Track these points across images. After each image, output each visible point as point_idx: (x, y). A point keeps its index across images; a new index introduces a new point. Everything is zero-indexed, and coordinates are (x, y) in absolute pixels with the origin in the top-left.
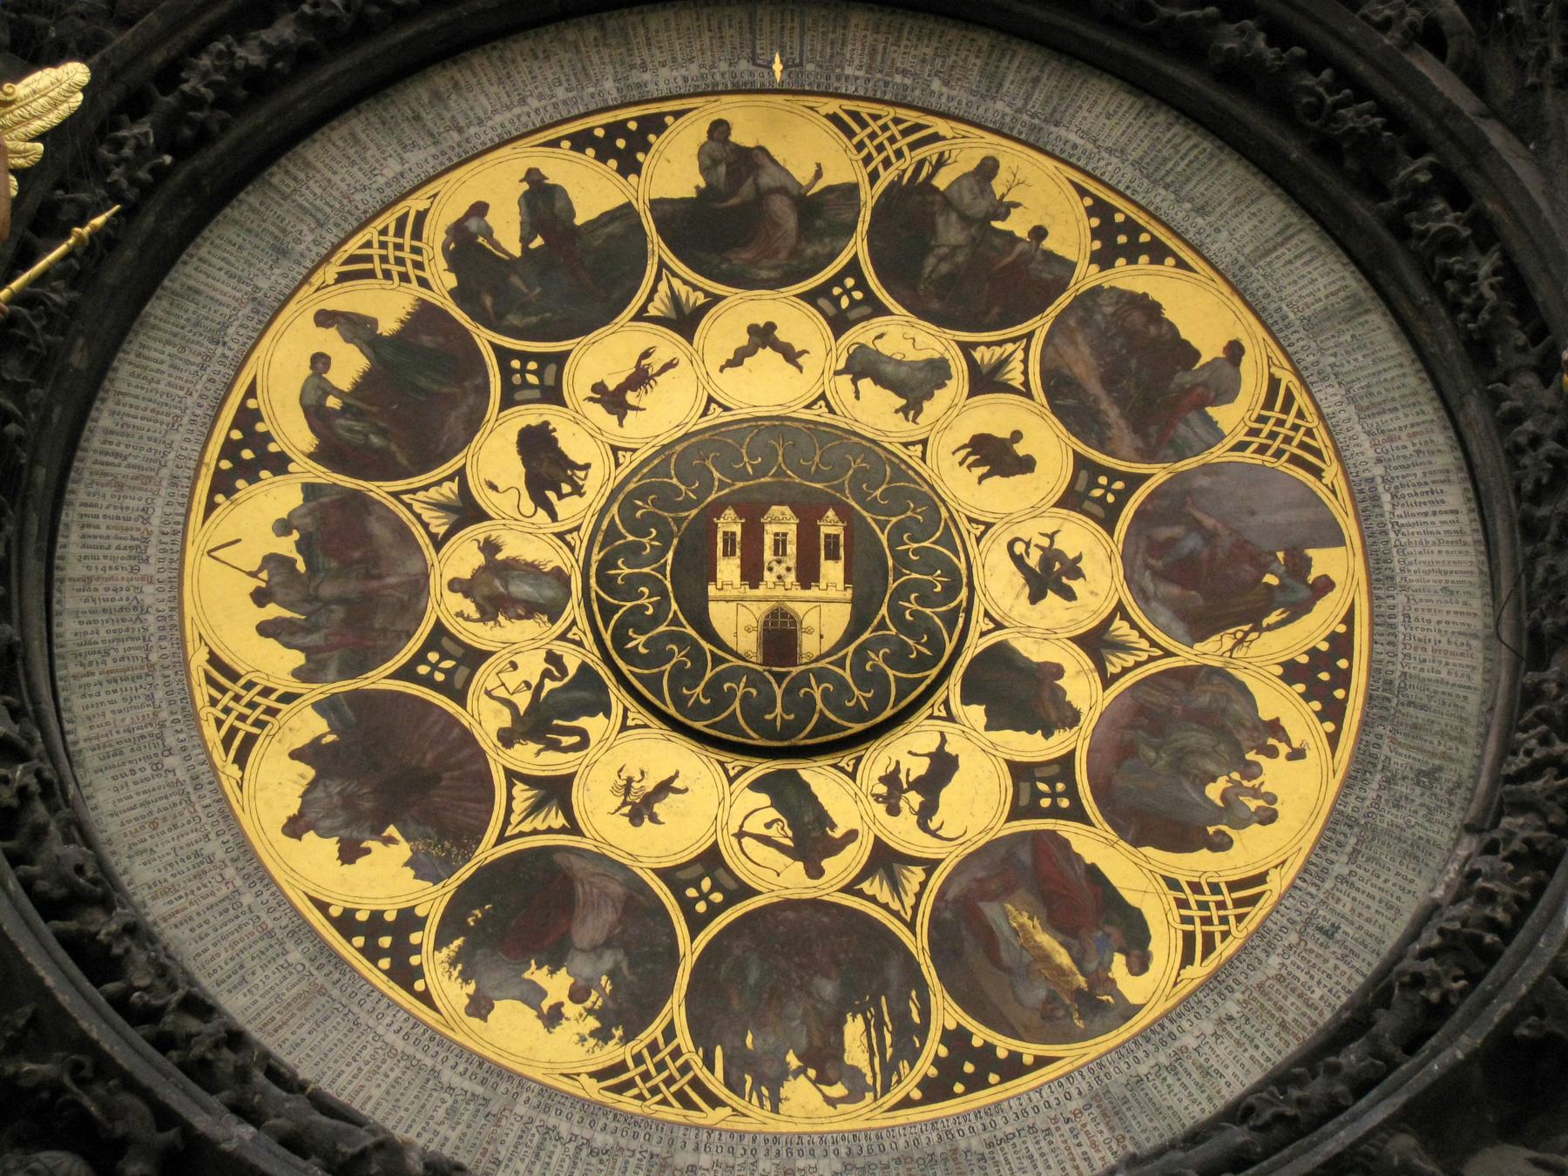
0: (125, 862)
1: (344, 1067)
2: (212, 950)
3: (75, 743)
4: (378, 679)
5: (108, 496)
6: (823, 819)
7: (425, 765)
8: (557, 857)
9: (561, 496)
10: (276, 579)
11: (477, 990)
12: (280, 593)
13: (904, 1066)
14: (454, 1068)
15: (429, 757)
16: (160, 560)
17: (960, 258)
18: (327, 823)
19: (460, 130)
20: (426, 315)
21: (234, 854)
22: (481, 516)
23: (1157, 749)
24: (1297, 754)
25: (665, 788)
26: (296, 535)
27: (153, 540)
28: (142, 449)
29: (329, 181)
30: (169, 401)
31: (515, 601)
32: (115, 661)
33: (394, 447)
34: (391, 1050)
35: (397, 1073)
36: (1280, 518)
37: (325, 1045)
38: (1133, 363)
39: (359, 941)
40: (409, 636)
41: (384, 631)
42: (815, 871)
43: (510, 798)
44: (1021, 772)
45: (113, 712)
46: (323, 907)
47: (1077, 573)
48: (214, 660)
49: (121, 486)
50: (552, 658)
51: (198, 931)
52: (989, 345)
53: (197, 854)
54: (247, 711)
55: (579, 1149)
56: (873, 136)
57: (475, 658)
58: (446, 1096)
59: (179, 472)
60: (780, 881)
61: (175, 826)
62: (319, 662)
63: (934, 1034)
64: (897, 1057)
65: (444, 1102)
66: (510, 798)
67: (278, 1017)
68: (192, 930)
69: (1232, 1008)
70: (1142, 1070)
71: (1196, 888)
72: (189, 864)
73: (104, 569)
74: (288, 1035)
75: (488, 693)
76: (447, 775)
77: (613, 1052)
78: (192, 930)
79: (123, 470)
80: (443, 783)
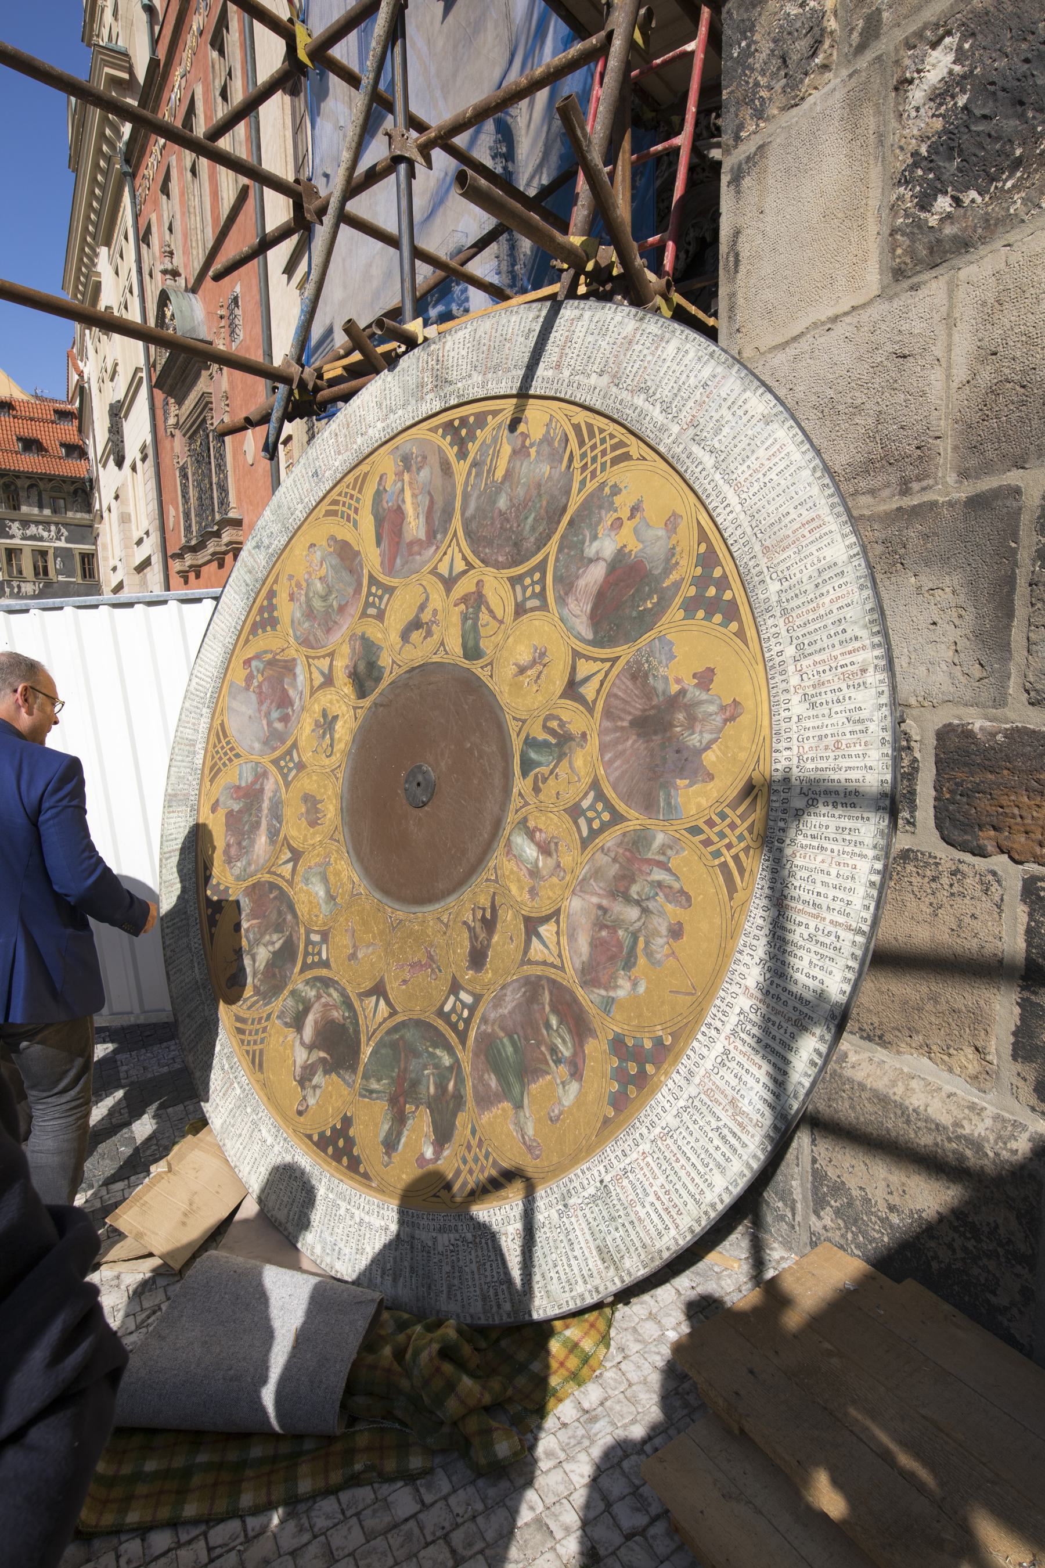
0: (877, 716)
1: (775, 478)
2: (834, 608)
3: (877, 858)
4: (635, 819)
5: (746, 1101)
6: (465, 618)
7: (634, 737)
8: (590, 636)
9: (484, 909)
10: (661, 941)
12: (663, 930)
13: (488, 442)
15: (630, 742)
17: (267, 937)
18: (712, 708)
20: (485, 1101)
21: (782, 697)
23: (331, 606)
24: (291, 577)
25: (522, 670)
26: (634, 972)
27: (727, 1030)
31: (538, 845)
32: (807, 926)
33: (547, 1008)
34: (738, 488)
35: (741, 469)
36: (243, 709)
37: (780, 500)
39: (728, 596)
40: (602, 848)
41: (615, 860)
42: (479, 583)
44: (380, 616)
45: (829, 873)
46: (741, 634)
47: (317, 725)
50: (537, 790)
52: (283, 877)
53: (813, 705)
54: (727, 831)
55: (654, 394)
56: (255, 1042)
57: (575, 812)
59: (683, 1083)
61: (820, 738)
62: (664, 854)
64: (489, 446)
65: (720, 441)
66: (598, 692)
68: (844, 631)
72: (823, 698)
73: (780, 1027)
76: (625, 724)
77: (616, 475)
78: (844, 631)
79: (726, 1119)
80: (630, 718)
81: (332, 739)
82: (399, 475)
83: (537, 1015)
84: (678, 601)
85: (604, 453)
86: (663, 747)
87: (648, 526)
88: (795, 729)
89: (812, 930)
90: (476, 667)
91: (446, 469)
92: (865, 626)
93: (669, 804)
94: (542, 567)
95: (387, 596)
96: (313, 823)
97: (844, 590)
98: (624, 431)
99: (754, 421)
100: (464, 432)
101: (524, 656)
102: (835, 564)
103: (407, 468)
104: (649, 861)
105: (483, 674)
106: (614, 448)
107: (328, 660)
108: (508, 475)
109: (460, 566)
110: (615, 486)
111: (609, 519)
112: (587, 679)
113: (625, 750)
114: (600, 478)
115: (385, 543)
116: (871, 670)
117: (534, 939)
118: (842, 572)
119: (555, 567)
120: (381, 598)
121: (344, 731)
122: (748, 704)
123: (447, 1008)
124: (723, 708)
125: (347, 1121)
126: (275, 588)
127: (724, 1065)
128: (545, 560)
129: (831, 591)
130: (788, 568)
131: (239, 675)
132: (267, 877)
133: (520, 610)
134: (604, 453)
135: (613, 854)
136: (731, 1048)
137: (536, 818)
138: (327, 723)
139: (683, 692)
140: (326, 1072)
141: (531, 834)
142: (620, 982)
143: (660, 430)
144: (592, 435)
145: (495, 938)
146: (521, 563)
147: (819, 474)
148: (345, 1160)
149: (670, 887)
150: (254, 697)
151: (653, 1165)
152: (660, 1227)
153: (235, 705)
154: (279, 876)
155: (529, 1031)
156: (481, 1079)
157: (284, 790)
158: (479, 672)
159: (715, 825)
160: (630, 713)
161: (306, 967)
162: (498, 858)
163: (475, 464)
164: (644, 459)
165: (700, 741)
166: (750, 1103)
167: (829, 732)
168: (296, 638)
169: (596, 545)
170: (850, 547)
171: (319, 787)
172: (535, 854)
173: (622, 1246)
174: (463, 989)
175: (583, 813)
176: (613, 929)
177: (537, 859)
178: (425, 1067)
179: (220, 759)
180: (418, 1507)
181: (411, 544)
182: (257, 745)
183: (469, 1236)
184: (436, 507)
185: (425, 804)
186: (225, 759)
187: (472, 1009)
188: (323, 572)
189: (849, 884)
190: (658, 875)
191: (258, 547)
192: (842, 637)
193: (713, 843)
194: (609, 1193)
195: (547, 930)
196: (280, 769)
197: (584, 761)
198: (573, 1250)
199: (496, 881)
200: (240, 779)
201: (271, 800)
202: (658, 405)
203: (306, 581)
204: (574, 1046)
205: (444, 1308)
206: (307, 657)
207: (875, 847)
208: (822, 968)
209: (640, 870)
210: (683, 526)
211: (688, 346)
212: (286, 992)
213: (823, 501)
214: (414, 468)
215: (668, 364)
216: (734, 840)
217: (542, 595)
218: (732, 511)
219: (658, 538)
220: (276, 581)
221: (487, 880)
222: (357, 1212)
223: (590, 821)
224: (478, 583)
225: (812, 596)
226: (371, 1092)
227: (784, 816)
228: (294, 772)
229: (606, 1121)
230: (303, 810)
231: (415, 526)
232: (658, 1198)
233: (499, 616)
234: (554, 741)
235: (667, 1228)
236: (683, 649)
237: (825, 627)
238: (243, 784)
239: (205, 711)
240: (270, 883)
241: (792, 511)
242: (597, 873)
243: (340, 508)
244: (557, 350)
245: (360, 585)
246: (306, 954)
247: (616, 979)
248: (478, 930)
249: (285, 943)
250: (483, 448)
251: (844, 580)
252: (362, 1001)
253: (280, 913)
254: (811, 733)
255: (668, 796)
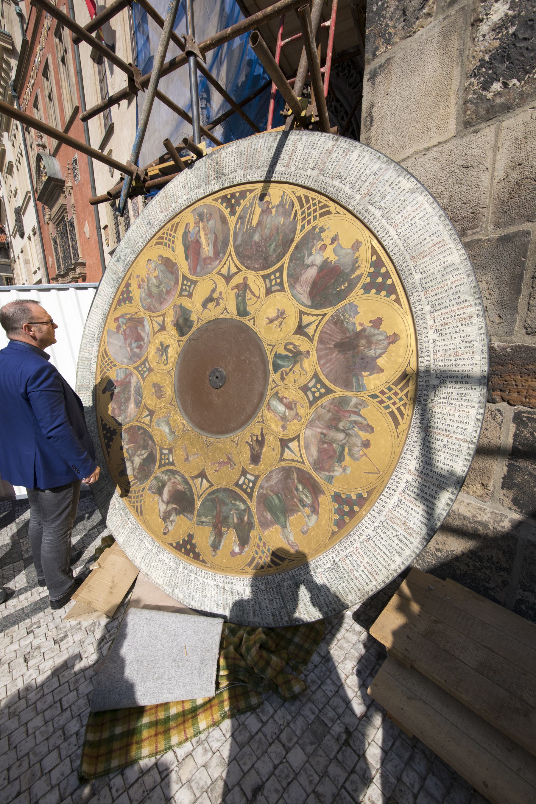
3: (480, 407)
4: (339, 392)
5: (412, 523)
6: (237, 296)
7: (337, 352)
8: (309, 303)
9: (257, 436)
10: (358, 449)
11: (354, 253)
12: (359, 443)
13: (247, 206)
14: (375, 217)
15: (335, 355)
16: (401, 479)
17: (139, 452)
18: (381, 337)
19: (224, 588)
20: (265, 525)
22: (281, 440)
23: (162, 291)
24: (138, 276)
25: (271, 321)
26: (343, 464)
27: (400, 490)
28: (388, 536)
29: (269, 602)
30: (367, 551)
32: (442, 441)
33: (296, 481)
34: (396, 227)
36: (116, 342)
37: (421, 232)
38: (123, 400)
39: (389, 282)
40: (321, 406)
41: (329, 411)
42: (245, 279)
43: (315, 331)
44: (190, 296)
46: (397, 301)
47: (158, 349)
48: (397, 423)
49: (404, 523)
50: (283, 379)
51: (457, 297)
52: (145, 424)
53: (442, 335)
54: (393, 396)
55: (345, 179)
56: (137, 502)
57: (305, 389)
58: (383, 205)
60: (254, 278)
61: (446, 350)
62: (357, 408)
63: (237, 215)
64: (248, 209)
66: (315, 331)
67: (436, 249)
68: (459, 297)
69: (173, 205)
70: (196, 191)
71: (169, 247)
73: (429, 488)
74: (435, 239)
75: (306, 374)
76: (331, 346)
77: (321, 222)
78: (459, 297)
79: (401, 531)
80: (334, 343)
81: (167, 356)
82: (197, 224)
83: (291, 485)
84: (360, 285)
85: (315, 211)
86: (353, 356)
87: (342, 248)
88: (431, 346)
89: (445, 442)
90: (245, 320)
91: (224, 220)
92: (471, 295)
93: (359, 384)
94: (281, 270)
95: (193, 286)
96: (160, 397)
97: (459, 277)
98: (327, 199)
99: (404, 192)
100: (233, 201)
101: (272, 314)
102: (453, 264)
103: (201, 220)
104: (348, 411)
105: (250, 324)
106: (321, 208)
107: (162, 318)
108: (259, 223)
109: (234, 270)
110: (322, 227)
111: (319, 245)
112: (309, 325)
113: (332, 359)
114: (313, 223)
115: (191, 258)
116: (475, 316)
117: (286, 449)
118: (458, 268)
119: (288, 270)
120: (190, 287)
121: (173, 352)
122: (403, 336)
123: (241, 482)
124: (388, 337)
125: (191, 537)
126: (129, 281)
127: (399, 506)
128: (282, 266)
129: (451, 278)
130: (426, 267)
131: (112, 325)
132: (136, 424)
133: (269, 292)
134: (315, 211)
135: (328, 409)
136: (402, 498)
137: (283, 392)
138: (164, 349)
139: (364, 330)
140: (177, 514)
141: (281, 400)
142: (336, 468)
143: (349, 198)
144: (308, 201)
145: (264, 449)
146: (269, 268)
147: (443, 219)
148: (191, 555)
149: (361, 423)
150: (122, 337)
151: (362, 553)
152: (367, 581)
153: (111, 340)
154: (143, 423)
155: (287, 492)
156: (262, 515)
157: (142, 382)
158: (247, 322)
159: (386, 393)
160: (334, 341)
161: (161, 466)
162: (263, 411)
163: (240, 218)
164: (339, 213)
165: (375, 354)
166: (414, 523)
167: (451, 347)
168: (143, 307)
169: (311, 258)
170: (462, 255)
171: (161, 379)
172: (284, 409)
173: (347, 590)
174: (249, 473)
175: (310, 389)
176: (330, 443)
177: (285, 411)
178: (231, 510)
179: (105, 367)
180: (260, 725)
181: (205, 259)
182: (125, 360)
183: (263, 588)
184: (218, 240)
185: (221, 387)
186: (108, 367)
187: (254, 483)
188: (156, 273)
189: (465, 420)
190: (354, 418)
191: (118, 261)
192: (458, 300)
193: (385, 402)
194: (338, 566)
195: (293, 445)
196: (139, 372)
197: (310, 364)
198: (320, 592)
199: (263, 422)
200: (117, 376)
201: (135, 386)
202: (348, 185)
203: (147, 278)
204: (312, 498)
205: (252, 620)
206: (150, 316)
207: (479, 402)
208: (451, 460)
209: (344, 416)
210: (362, 248)
211: (365, 154)
212: (152, 478)
213: (446, 233)
214: (205, 220)
215: (353, 163)
216: (397, 401)
217: (281, 284)
218: (392, 238)
219: (348, 254)
220: (130, 278)
221: (258, 422)
222: (201, 579)
223: (313, 393)
224: (244, 279)
225: (440, 280)
226: (203, 522)
227: (427, 388)
228: (147, 373)
229: (334, 533)
230: (154, 391)
231: (207, 250)
232: (366, 568)
233: (257, 295)
234: (291, 355)
235: (371, 581)
236: (364, 308)
237: (448, 296)
238: (119, 379)
239: (95, 344)
240: (138, 426)
241: (428, 238)
242: (319, 418)
243: (164, 241)
244: (287, 157)
245: (177, 280)
246: (161, 459)
247: (333, 467)
248: (255, 445)
249: (149, 454)
250: (245, 209)
251: (459, 272)
252: (193, 480)
253: (145, 440)
254: (441, 348)
255: (358, 380)
